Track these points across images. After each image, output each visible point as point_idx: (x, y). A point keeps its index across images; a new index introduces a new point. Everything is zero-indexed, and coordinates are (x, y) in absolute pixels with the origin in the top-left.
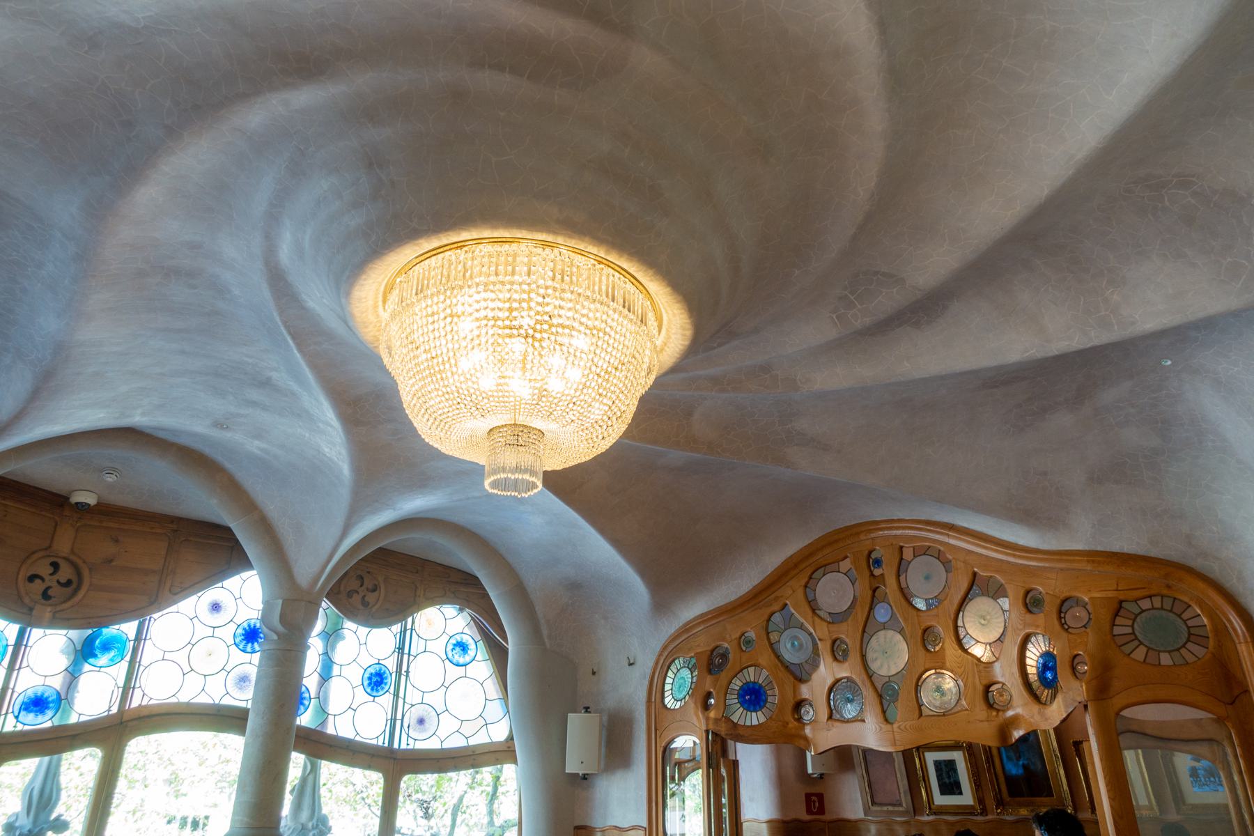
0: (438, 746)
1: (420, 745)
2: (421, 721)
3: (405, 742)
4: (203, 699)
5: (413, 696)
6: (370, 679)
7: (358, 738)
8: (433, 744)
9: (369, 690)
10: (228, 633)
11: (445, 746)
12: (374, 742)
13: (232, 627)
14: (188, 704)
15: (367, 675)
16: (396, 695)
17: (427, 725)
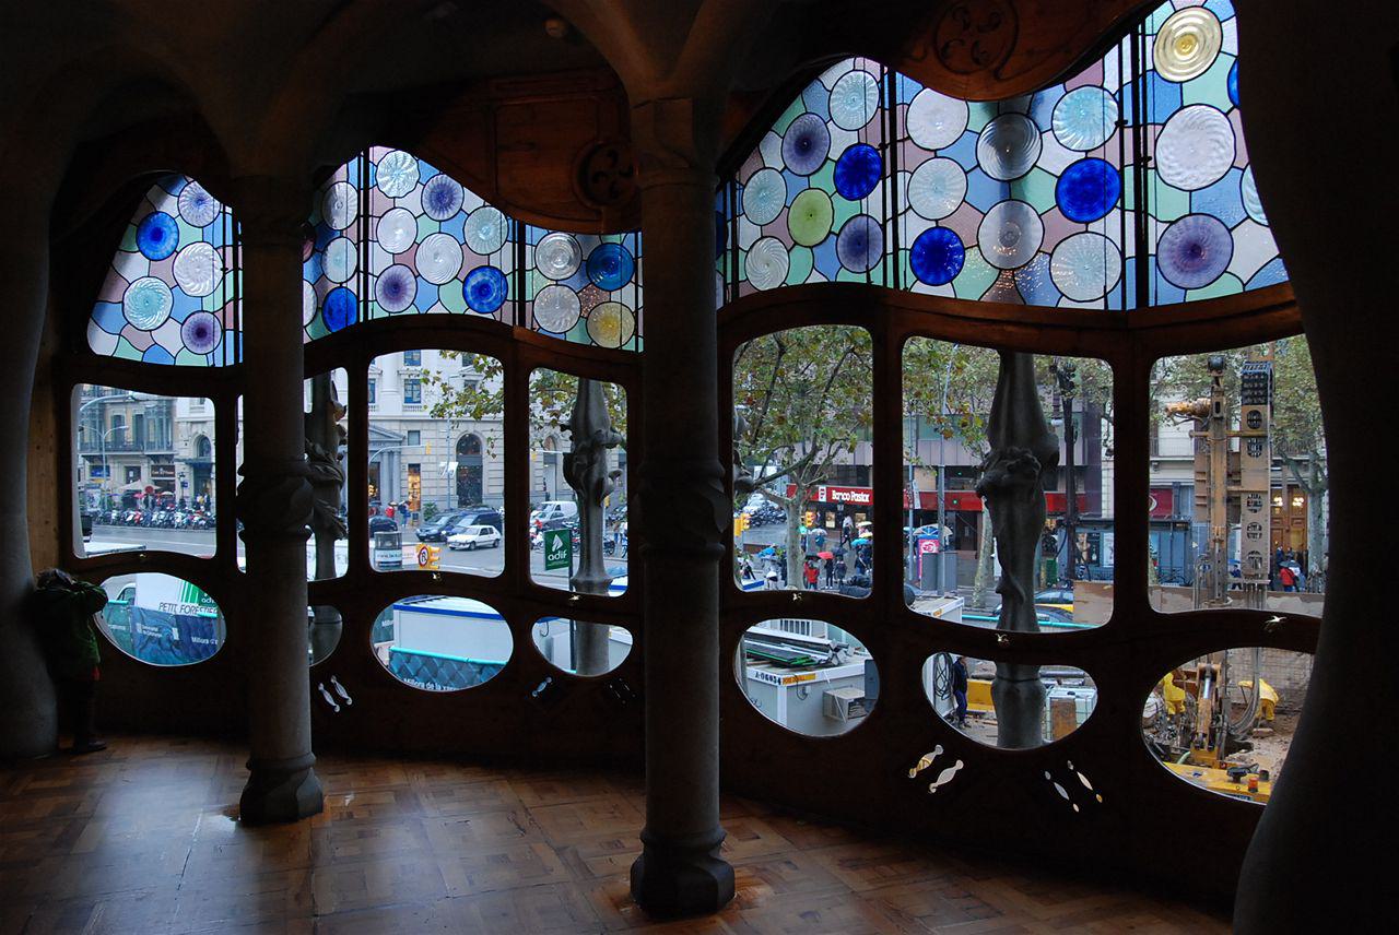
0: (1238, 289)
1: (1193, 296)
2: (1193, 253)
3: (1164, 293)
4: (816, 278)
5: (1166, 204)
6: (1069, 191)
7: (1065, 303)
8: (1226, 287)
9: (1072, 213)
10: (826, 178)
11: (1247, 289)
12: (1100, 305)
13: (830, 168)
14: (804, 287)
15: (1064, 186)
16: (1141, 213)
17: (1205, 255)
